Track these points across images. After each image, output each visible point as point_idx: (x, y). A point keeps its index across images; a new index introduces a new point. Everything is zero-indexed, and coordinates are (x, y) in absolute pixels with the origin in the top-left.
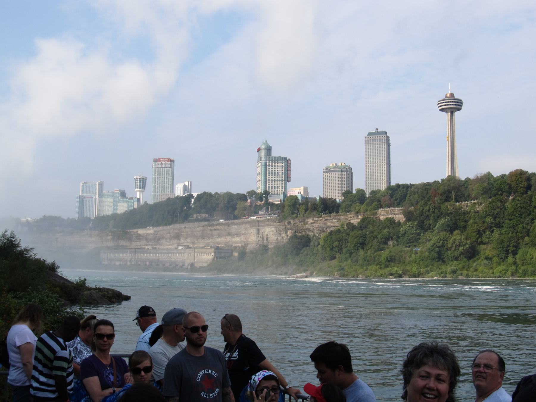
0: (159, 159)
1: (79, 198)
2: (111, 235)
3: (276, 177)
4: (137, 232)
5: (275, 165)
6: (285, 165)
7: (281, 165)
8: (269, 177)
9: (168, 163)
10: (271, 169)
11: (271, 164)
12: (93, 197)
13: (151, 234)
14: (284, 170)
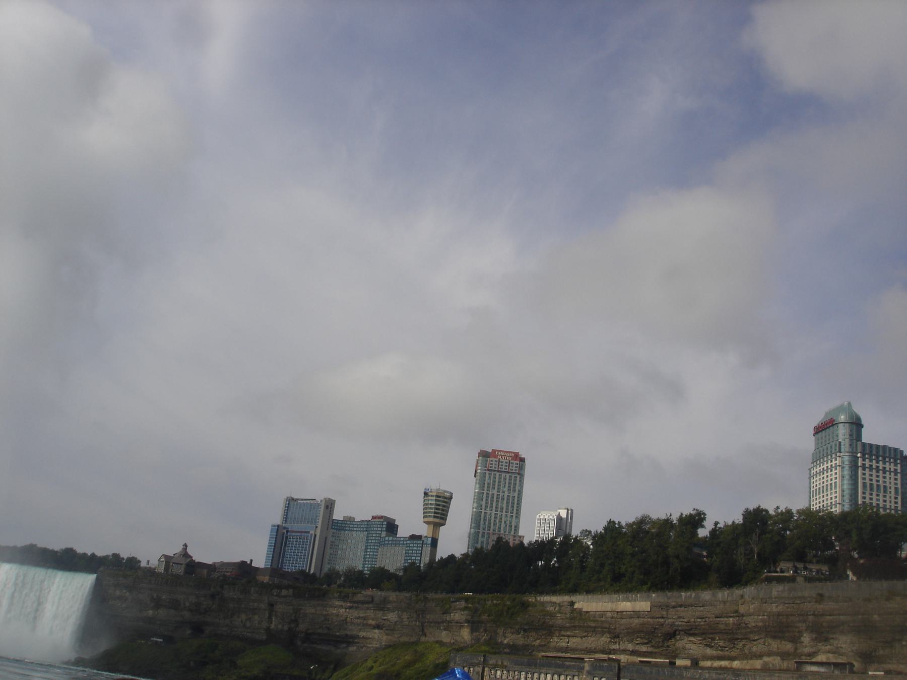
0: (494, 451)
1: (278, 530)
2: (466, 608)
3: (881, 498)
4: (572, 604)
5: (878, 467)
6: (902, 471)
7: (892, 470)
8: (864, 498)
9: (515, 462)
10: (867, 476)
11: (867, 463)
12: (309, 532)
13: (636, 614)
14: (899, 482)
